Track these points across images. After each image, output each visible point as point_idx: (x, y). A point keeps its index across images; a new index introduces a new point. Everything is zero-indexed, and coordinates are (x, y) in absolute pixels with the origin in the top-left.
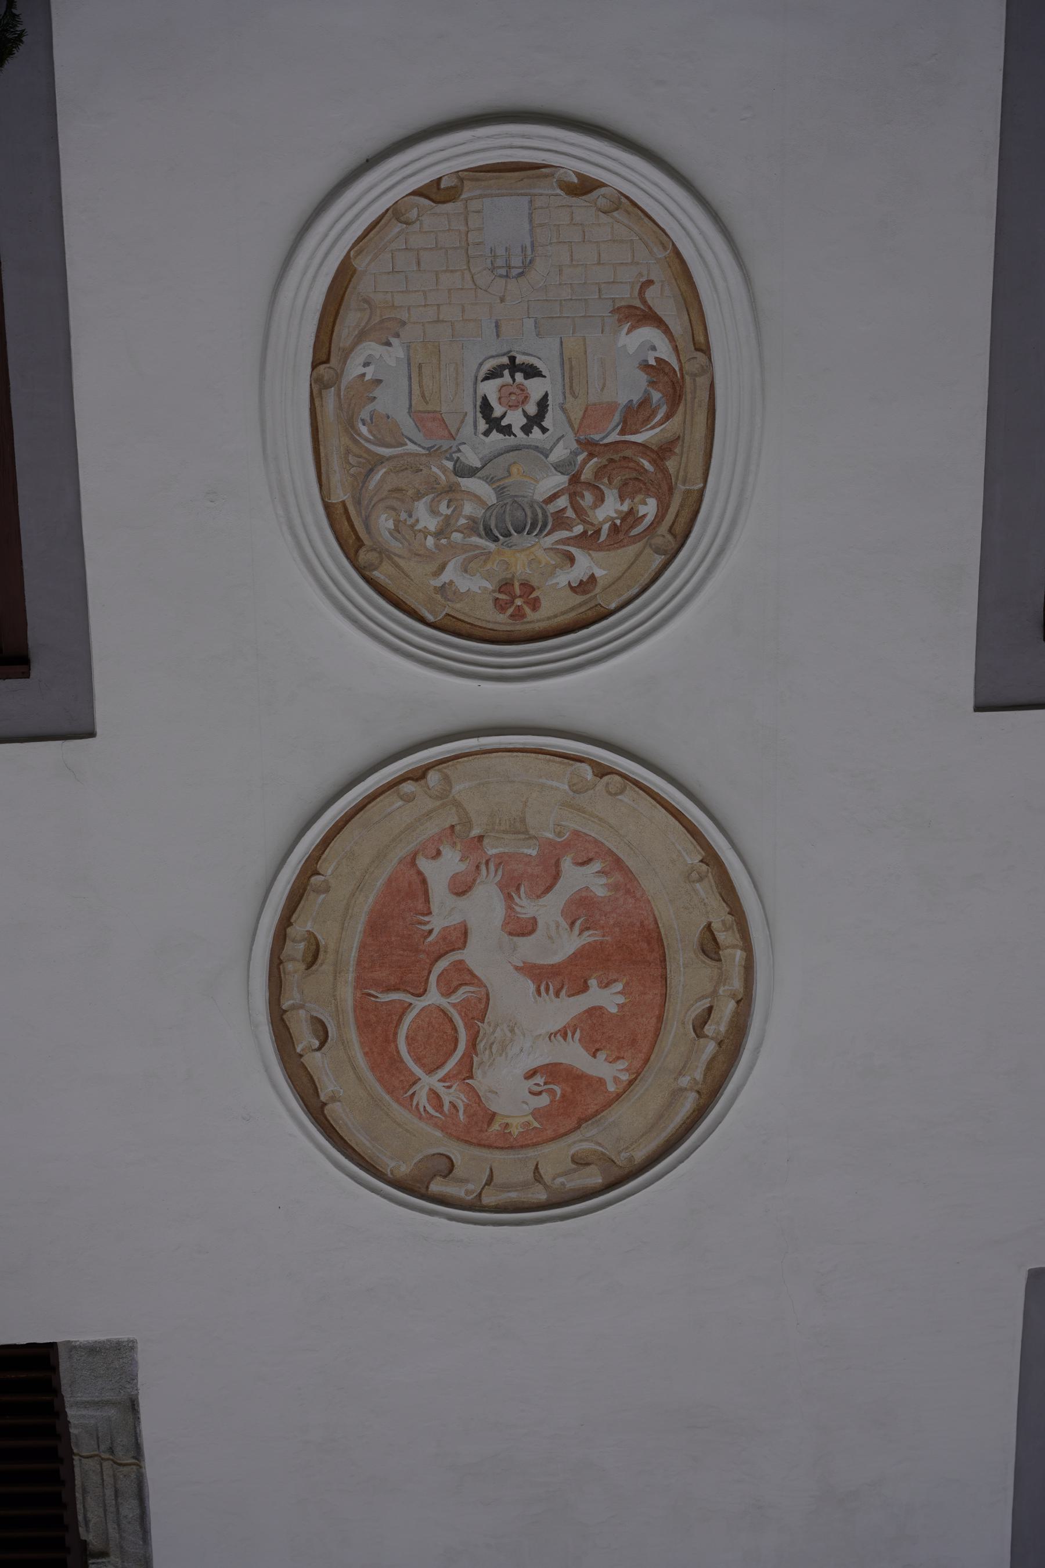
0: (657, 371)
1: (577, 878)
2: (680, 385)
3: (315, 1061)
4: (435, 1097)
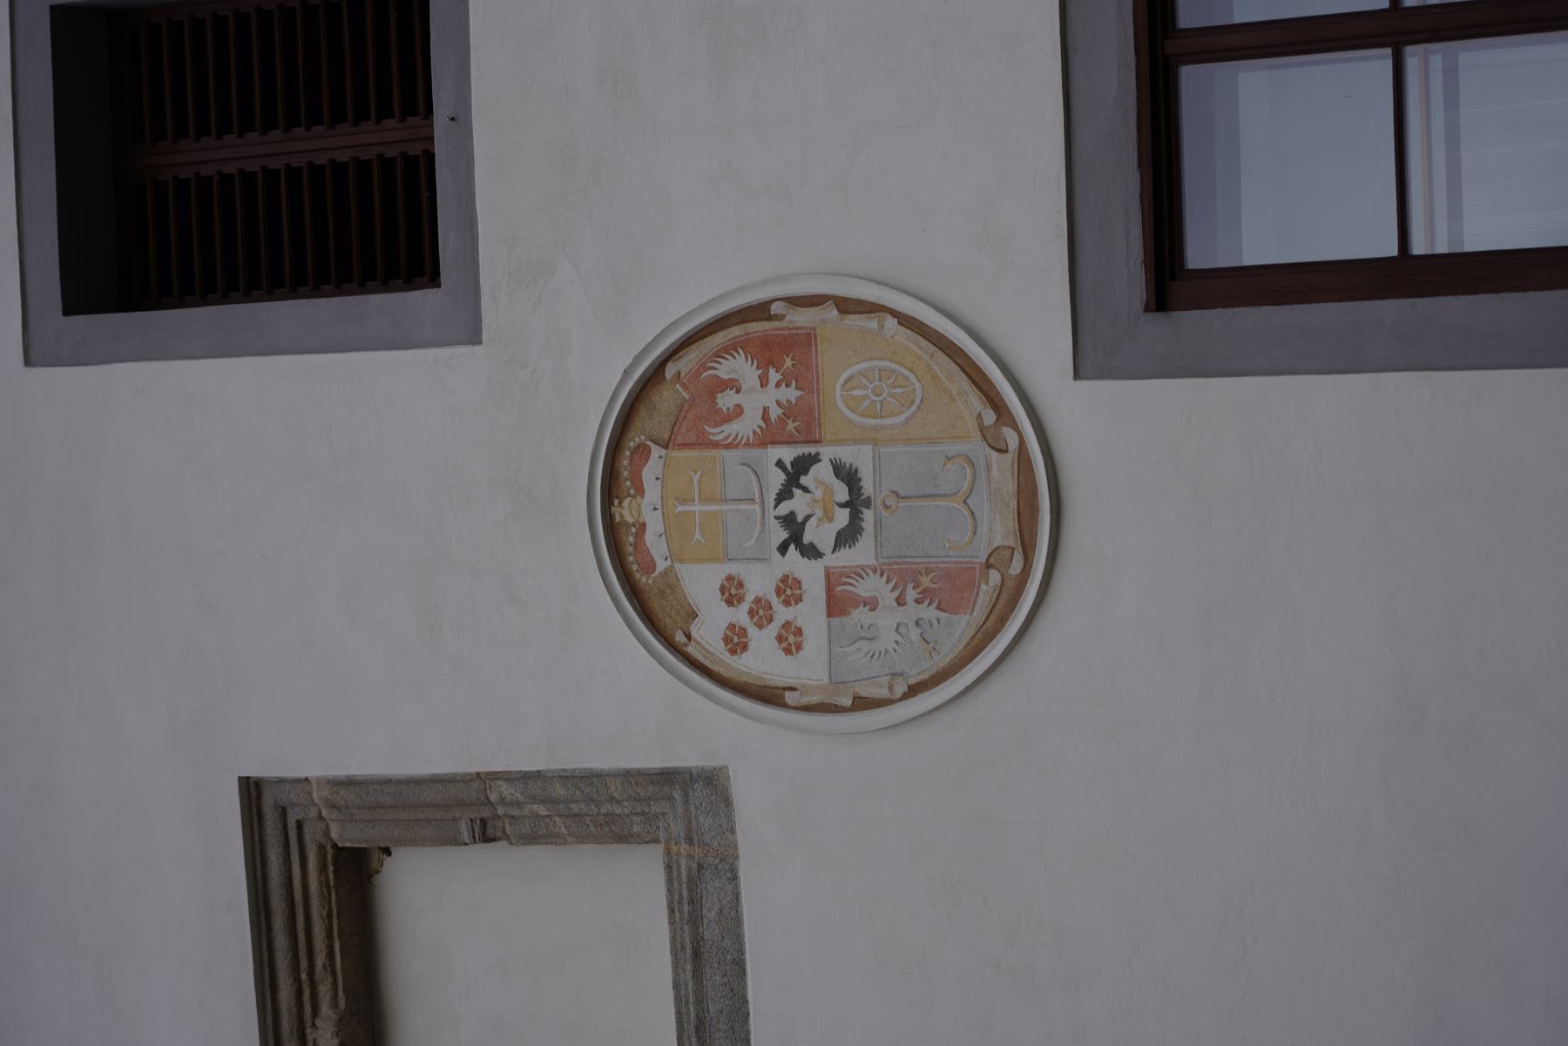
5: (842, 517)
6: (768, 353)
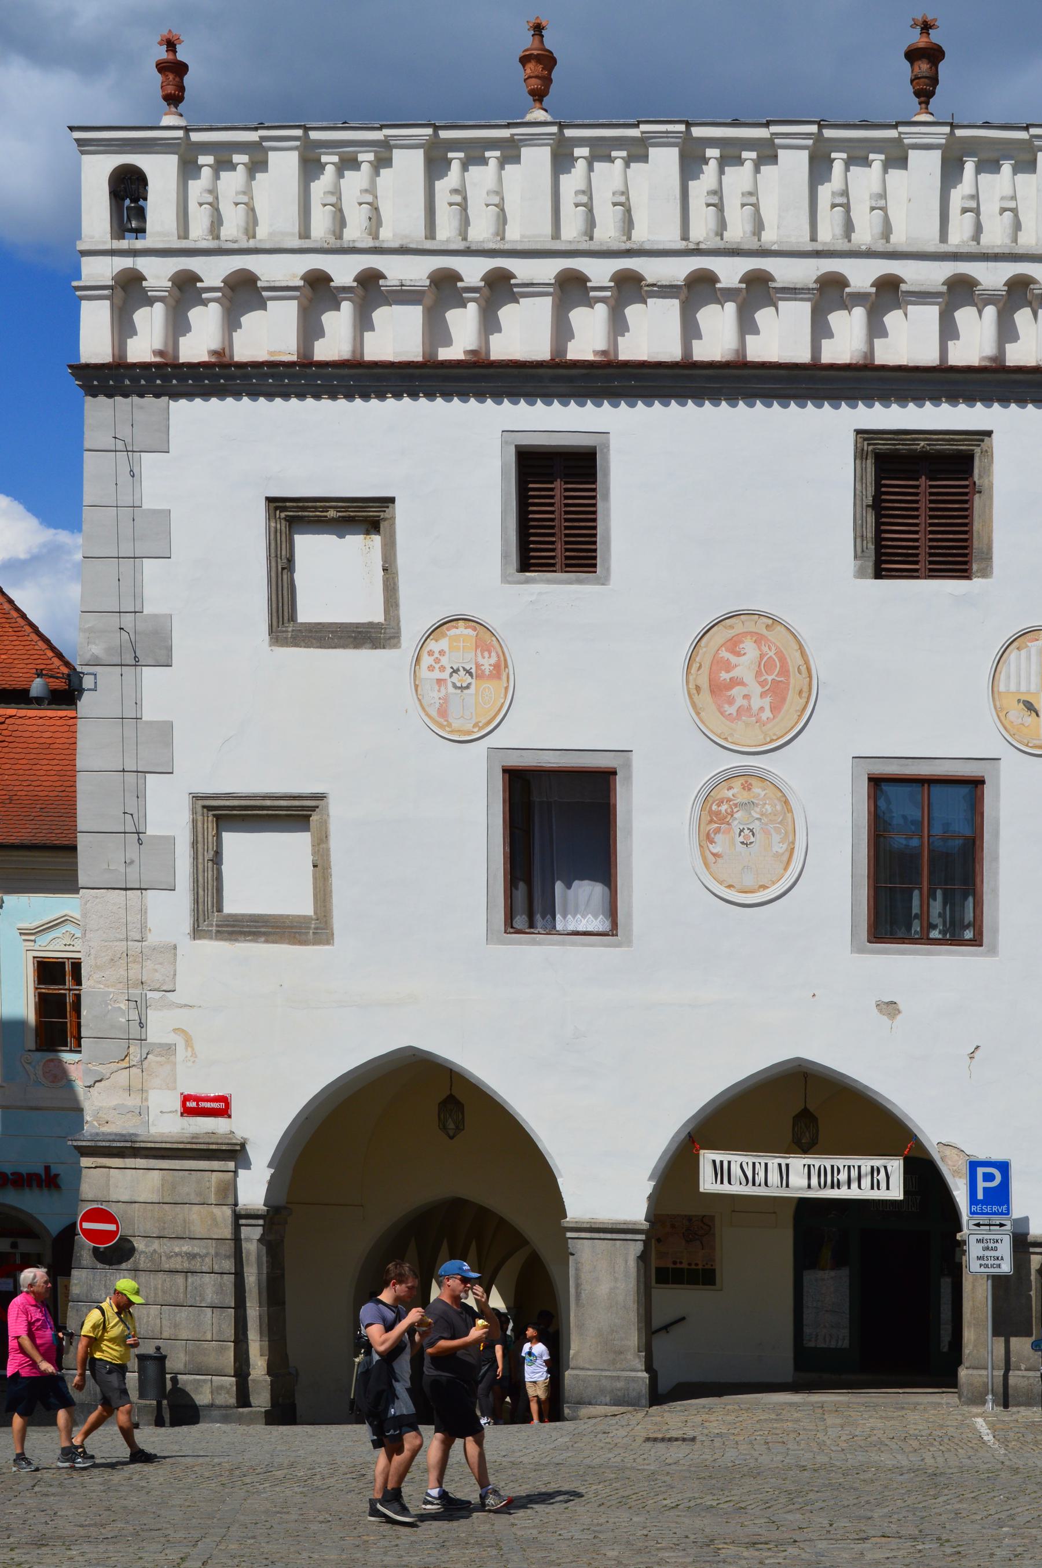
0: (712, 842)
1: (732, 710)
3: (801, 662)
4: (770, 649)
5: (459, 685)
6: (497, 666)
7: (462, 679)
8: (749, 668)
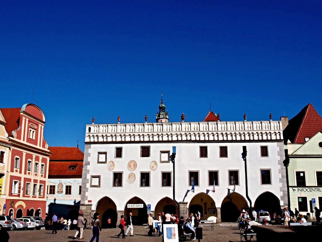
2: (129, 178)
7: (111, 166)
8: (133, 165)
